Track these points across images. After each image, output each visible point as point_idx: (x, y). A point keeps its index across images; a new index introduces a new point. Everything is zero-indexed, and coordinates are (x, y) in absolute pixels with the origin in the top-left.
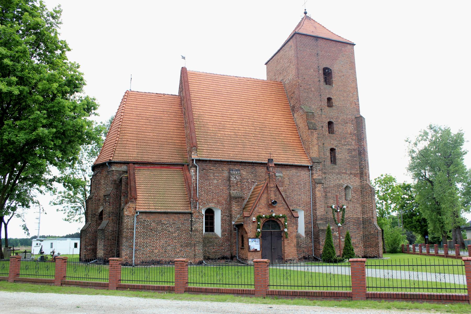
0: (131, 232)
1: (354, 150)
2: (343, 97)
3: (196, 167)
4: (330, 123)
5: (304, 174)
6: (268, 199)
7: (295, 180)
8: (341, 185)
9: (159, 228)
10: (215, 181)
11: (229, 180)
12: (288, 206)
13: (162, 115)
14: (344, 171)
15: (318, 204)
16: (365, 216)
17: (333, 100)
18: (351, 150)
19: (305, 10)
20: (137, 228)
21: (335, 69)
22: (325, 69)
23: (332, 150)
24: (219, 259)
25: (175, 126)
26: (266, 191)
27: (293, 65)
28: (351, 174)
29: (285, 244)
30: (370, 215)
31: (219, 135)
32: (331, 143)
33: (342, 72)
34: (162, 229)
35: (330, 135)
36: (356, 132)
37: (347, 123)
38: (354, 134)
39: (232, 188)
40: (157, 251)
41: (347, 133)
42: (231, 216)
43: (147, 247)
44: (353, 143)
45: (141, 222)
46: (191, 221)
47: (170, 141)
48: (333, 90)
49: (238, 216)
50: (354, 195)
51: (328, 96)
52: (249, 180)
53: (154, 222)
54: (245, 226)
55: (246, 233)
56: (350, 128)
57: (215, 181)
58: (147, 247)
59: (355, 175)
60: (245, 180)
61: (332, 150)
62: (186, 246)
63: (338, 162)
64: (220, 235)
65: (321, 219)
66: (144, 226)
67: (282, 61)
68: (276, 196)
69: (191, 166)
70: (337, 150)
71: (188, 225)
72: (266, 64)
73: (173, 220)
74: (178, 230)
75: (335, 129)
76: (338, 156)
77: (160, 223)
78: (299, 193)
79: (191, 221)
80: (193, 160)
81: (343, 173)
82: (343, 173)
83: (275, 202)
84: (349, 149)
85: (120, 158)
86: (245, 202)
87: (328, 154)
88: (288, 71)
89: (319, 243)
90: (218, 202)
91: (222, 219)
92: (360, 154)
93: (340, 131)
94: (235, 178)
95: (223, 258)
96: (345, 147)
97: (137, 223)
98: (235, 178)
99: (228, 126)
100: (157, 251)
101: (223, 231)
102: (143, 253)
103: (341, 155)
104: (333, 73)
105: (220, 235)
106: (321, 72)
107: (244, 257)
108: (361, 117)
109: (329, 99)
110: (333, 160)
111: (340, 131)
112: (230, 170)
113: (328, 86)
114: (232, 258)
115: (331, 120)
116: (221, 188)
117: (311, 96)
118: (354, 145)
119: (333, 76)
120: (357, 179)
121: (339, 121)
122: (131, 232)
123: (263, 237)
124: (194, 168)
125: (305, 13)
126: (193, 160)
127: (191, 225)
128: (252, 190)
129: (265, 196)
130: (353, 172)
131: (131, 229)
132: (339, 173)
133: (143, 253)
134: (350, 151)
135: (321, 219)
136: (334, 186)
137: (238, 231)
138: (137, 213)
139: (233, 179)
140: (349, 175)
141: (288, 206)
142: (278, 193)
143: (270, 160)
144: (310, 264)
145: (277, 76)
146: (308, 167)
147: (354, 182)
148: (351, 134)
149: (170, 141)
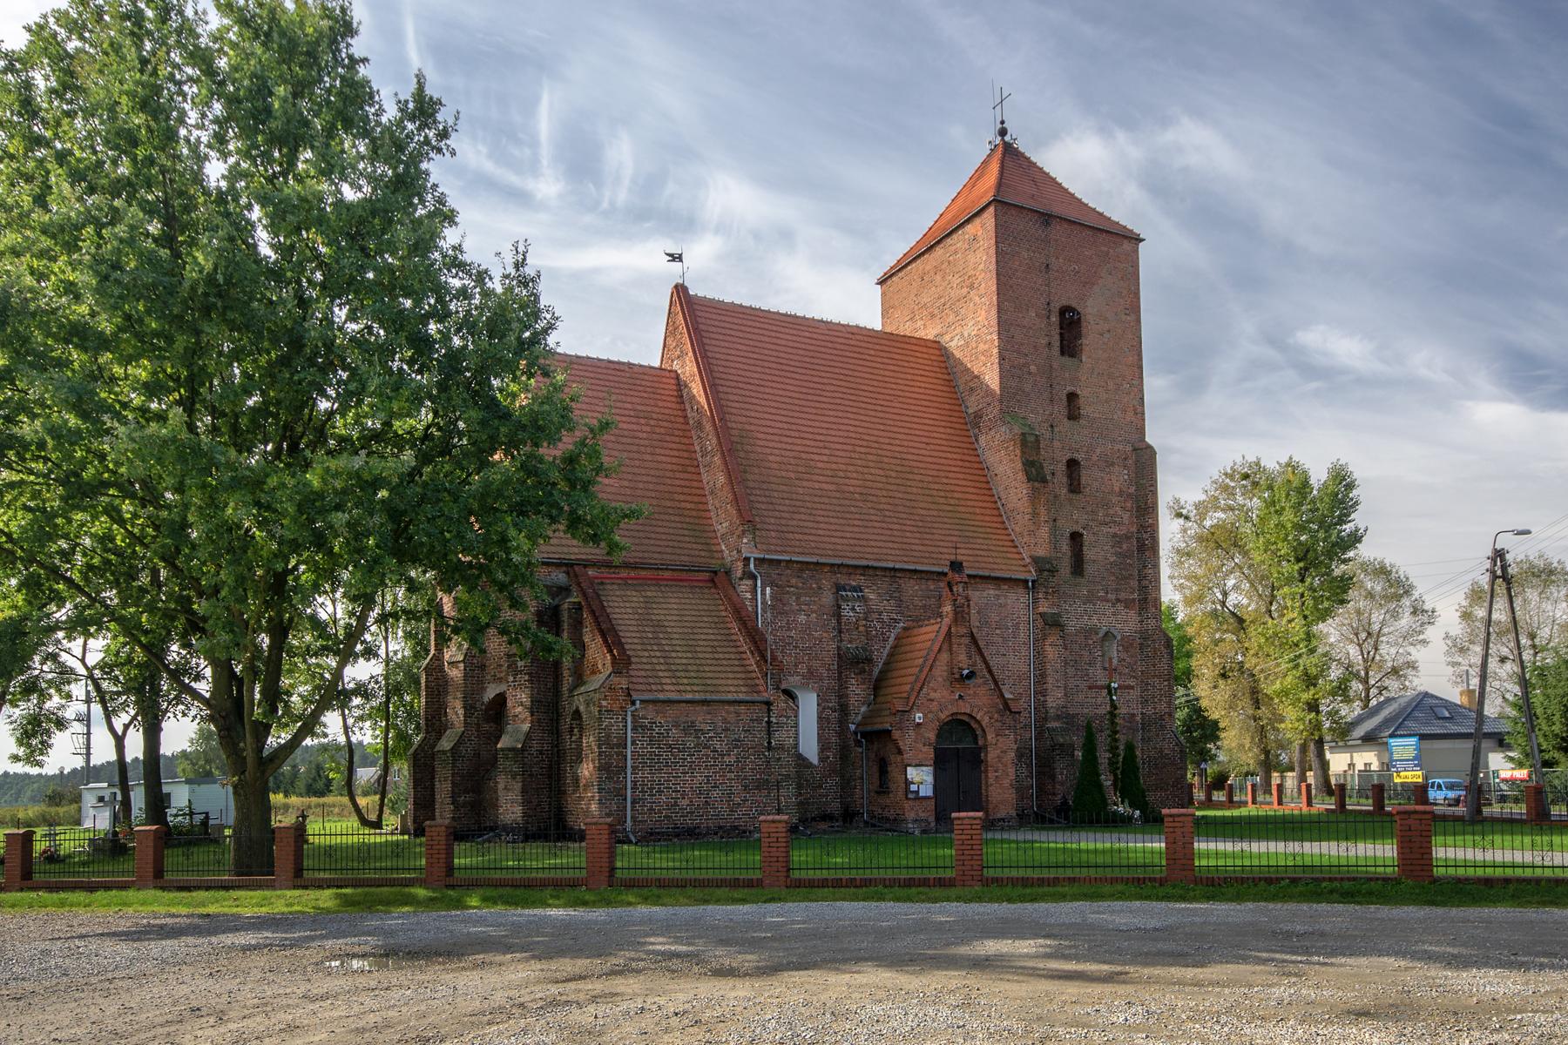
0: (618, 754)
1: (1128, 538)
2: (1107, 391)
3: (755, 578)
4: (1072, 464)
5: (1016, 601)
6: (951, 665)
7: (994, 617)
8: (1094, 630)
9: (691, 742)
10: (802, 618)
11: (839, 616)
12: (996, 683)
13: (635, 427)
14: (1101, 594)
15: (1050, 680)
16: (1150, 711)
17: (1081, 401)
18: (1120, 537)
19: (1002, 122)
20: (633, 743)
21: (1092, 309)
22: (1064, 311)
23: (1076, 537)
24: (814, 819)
25: (674, 460)
26: (945, 646)
27: (981, 297)
28: (1118, 600)
29: (991, 781)
30: (1163, 707)
31: (801, 491)
32: (1073, 519)
33: (1106, 319)
34: (697, 745)
35: (1073, 496)
36: (1132, 490)
37: (1113, 464)
38: (1129, 495)
39: (845, 636)
40: (685, 802)
41: (1112, 492)
42: (844, 709)
43: (660, 791)
44: (1126, 516)
45: (643, 727)
46: (769, 722)
47: (669, 504)
48: (1087, 375)
49: (863, 709)
50: (1124, 655)
51: (1070, 389)
52: (885, 616)
53: (676, 725)
54: (896, 734)
55: (900, 752)
56: (1119, 479)
57: (802, 618)
58: (660, 791)
59: (1128, 604)
60: (876, 616)
61: (1076, 537)
62: (758, 788)
63: (1089, 569)
64: (815, 760)
65: (1058, 718)
66: (651, 738)
67: (938, 277)
68: (970, 658)
69: (739, 573)
70: (1088, 538)
71: (760, 735)
72: (881, 282)
73: (725, 721)
74: (737, 747)
75: (1083, 481)
76: (1089, 553)
77: (690, 728)
78: (1002, 651)
79: (769, 722)
80: (747, 560)
81: (1099, 598)
82: (1099, 598)
83: (971, 675)
84: (1115, 535)
85: (559, 549)
86: (876, 671)
87: (1065, 547)
88: (963, 311)
89: (1053, 777)
90: (811, 674)
91: (819, 718)
92: (1142, 547)
93: (1096, 484)
94: (853, 609)
95: (826, 817)
96: (1105, 529)
97: (634, 729)
98: (853, 609)
99: (820, 465)
100: (685, 802)
101: (824, 748)
102: (651, 809)
103: (1098, 552)
104: (1084, 324)
105: (815, 760)
106: (1054, 319)
107: (891, 814)
108: (1150, 447)
109: (1072, 397)
110: (1078, 566)
111: (1096, 484)
112: (839, 588)
113: (1066, 360)
114: (849, 816)
115: (1076, 456)
116: (816, 634)
117: (1028, 387)
118: (1126, 520)
119: (1084, 331)
120: (1133, 615)
121: (1095, 458)
122: (618, 754)
123: (941, 762)
124: (749, 582)
125: (1003, 132)
126: (747, 560)
127: (769, 734)
128: (891, 640)
129: (945, 656)
130: (1123, 596)
131: (618, 746)
132: (1090, 599)
133: (651, 809)
134: (1117, 540)
135: (1058, 718)
136: (1078, 632)
137: (866, 745)
138: (633, 703)
139: (847, 612)
140: (1114, 605)
141: (996, 683)
142: (973, 649)
143: (956, 566)
144: (1048, 829)
145: (920, 323)
146: (1026, 581)
147: (1126, 623)
148: (1121, 493)
149: (669, 504)
